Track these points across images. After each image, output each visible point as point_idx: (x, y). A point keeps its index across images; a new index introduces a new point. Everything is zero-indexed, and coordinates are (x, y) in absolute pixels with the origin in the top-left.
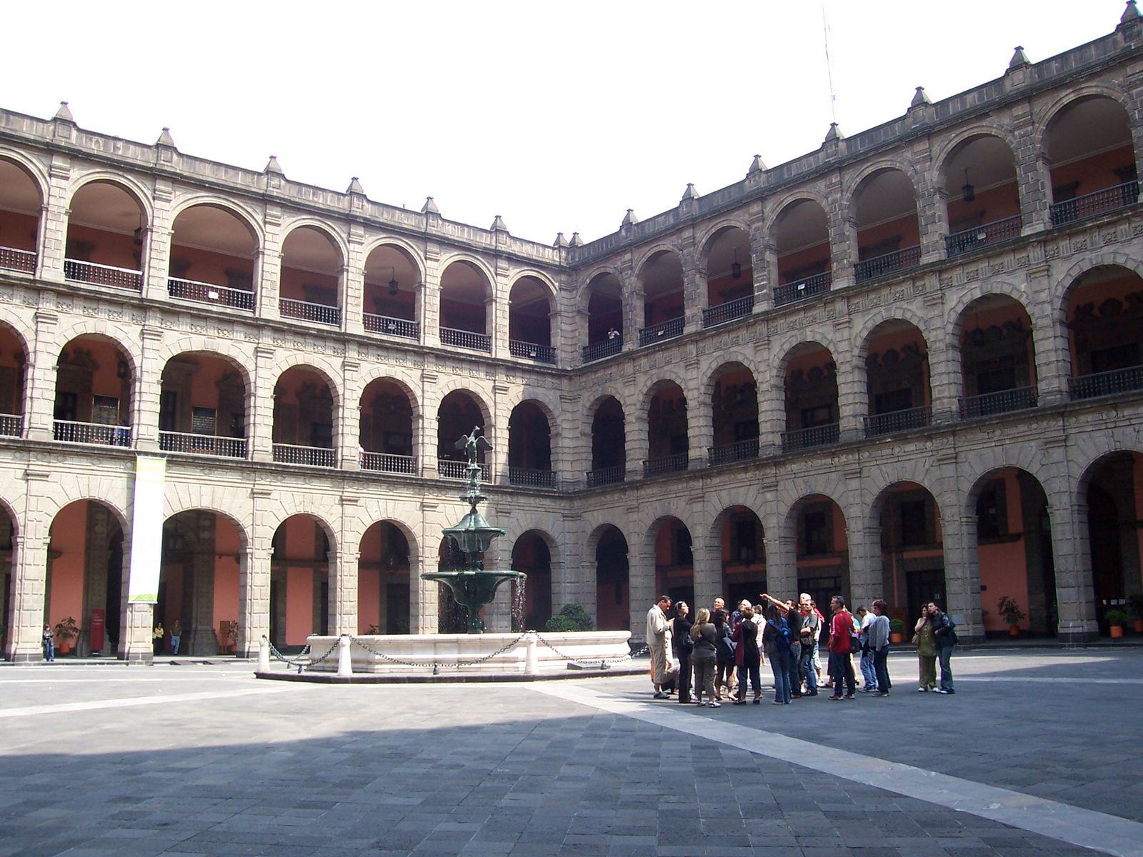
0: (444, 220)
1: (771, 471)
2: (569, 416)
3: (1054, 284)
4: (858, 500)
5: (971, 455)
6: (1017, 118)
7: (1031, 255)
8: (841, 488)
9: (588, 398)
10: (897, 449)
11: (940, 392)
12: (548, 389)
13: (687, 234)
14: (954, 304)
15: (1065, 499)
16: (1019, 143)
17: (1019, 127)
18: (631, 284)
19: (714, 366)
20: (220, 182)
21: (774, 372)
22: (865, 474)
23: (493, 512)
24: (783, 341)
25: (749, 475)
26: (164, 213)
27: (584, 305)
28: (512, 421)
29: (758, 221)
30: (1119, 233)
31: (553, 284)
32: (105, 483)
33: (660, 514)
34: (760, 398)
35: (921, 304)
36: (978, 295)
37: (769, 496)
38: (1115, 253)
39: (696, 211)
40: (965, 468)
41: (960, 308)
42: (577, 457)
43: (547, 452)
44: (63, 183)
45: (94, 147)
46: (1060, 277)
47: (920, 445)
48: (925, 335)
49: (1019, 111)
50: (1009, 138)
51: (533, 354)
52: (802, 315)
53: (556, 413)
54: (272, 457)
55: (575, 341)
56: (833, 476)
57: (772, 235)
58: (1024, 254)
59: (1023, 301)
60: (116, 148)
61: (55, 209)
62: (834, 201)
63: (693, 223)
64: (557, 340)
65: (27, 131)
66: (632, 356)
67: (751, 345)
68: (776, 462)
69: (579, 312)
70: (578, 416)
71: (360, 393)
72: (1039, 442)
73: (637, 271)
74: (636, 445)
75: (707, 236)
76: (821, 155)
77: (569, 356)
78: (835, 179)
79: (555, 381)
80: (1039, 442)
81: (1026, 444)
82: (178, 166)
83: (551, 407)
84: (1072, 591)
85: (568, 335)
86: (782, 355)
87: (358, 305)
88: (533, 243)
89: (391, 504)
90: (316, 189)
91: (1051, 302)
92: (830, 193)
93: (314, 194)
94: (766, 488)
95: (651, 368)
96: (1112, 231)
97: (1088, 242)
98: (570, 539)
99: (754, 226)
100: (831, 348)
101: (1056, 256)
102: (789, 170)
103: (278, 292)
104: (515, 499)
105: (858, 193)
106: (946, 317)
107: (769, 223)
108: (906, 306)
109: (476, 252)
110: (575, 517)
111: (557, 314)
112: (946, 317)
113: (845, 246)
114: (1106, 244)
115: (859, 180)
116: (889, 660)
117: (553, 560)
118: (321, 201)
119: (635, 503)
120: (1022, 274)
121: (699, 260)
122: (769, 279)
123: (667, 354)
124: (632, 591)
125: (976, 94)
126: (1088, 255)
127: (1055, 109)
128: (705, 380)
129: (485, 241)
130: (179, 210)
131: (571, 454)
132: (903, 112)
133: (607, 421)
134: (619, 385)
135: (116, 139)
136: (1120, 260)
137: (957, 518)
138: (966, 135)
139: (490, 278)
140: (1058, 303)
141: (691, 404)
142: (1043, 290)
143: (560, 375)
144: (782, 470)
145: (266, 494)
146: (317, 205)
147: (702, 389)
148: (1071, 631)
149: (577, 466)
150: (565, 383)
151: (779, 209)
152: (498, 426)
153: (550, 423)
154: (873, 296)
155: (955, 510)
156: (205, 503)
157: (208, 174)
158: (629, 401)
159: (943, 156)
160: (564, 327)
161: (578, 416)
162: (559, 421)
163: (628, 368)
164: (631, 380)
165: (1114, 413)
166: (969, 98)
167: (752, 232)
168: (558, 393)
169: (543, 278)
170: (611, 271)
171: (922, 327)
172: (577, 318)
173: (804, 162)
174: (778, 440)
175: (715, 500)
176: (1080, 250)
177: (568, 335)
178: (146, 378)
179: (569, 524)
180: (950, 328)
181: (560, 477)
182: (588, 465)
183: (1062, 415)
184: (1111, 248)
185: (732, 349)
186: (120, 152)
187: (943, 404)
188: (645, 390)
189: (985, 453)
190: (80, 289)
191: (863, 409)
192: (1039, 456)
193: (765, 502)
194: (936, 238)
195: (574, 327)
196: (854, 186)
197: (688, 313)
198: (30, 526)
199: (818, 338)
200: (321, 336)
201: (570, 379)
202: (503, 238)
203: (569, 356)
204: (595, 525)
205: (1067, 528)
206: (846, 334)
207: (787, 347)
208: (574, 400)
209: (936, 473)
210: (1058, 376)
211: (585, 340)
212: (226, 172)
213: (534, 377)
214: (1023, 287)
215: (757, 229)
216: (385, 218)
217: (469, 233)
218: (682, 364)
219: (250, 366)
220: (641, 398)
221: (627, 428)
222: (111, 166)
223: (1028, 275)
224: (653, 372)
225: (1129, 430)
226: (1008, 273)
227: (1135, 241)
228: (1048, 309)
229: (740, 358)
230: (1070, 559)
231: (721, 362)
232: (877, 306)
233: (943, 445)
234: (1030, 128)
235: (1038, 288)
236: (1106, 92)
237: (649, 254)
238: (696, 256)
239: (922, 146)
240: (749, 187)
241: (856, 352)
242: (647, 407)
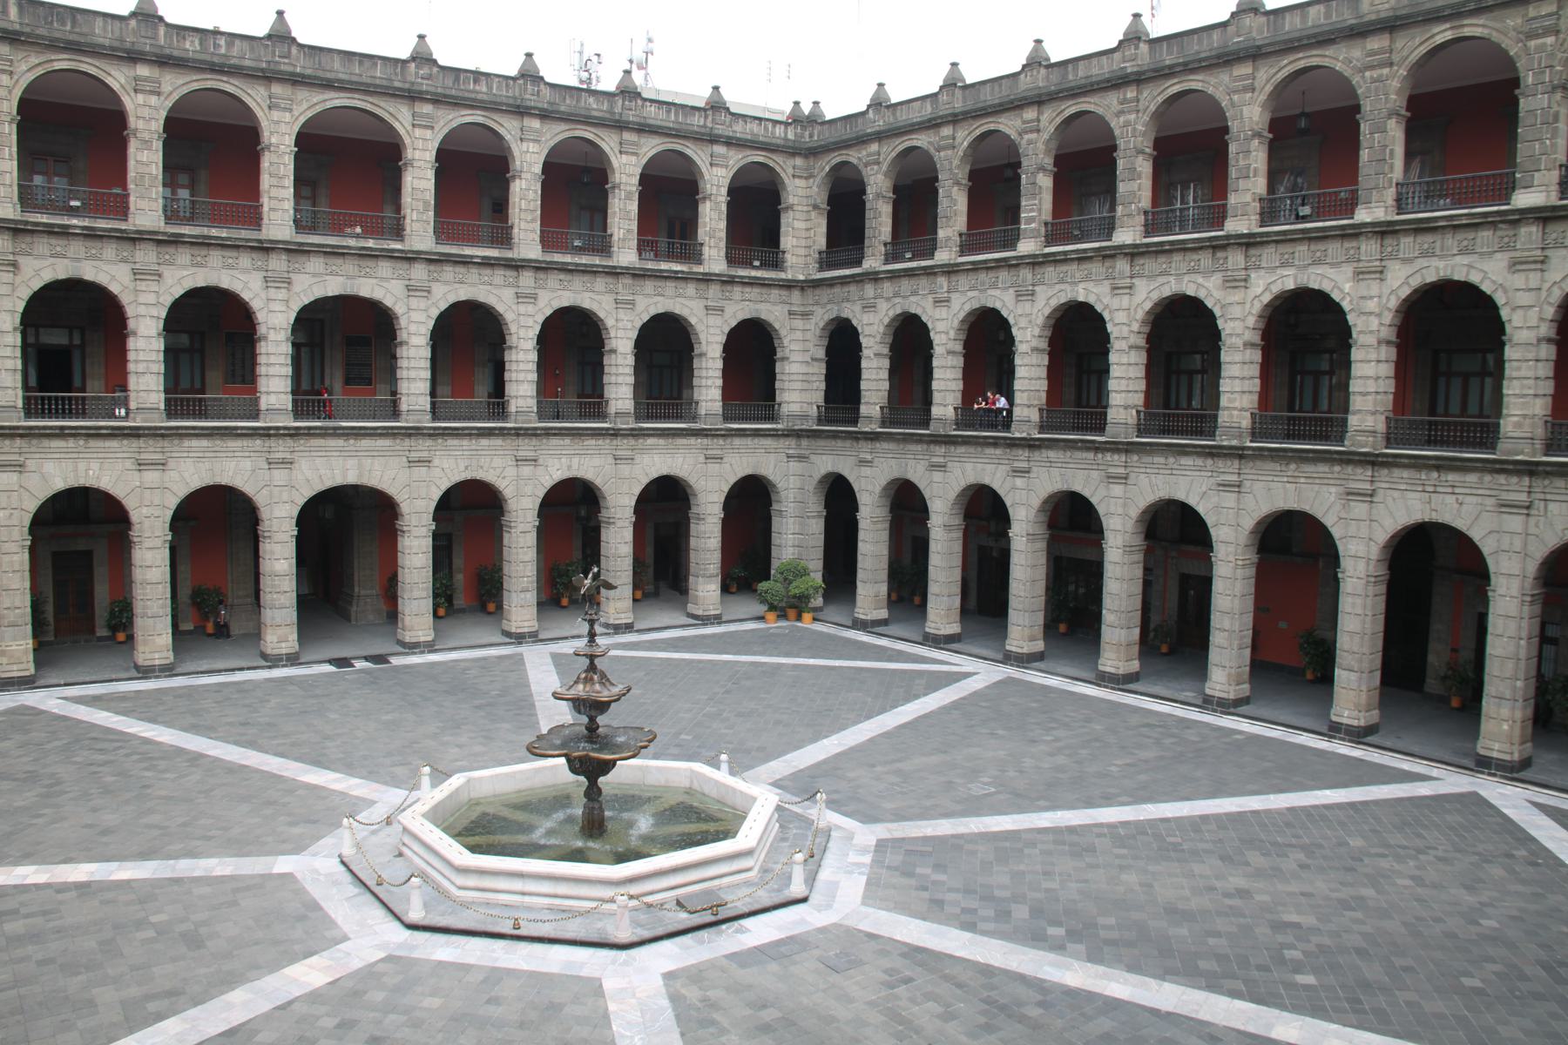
0: (646, 100)
1: (1023, 454)
2: (799, 335)
3: (1386, 291)
4: (1120, 511)
6: (1372, 53)
7: (1363, 248)
8: (1102, 492)
9: (822, 316)
10: (1171, 460)
11: (1230, 400)
12: (774, 304)
13: (946, 131)
14: (1259, 290)
15: (1361, 566)
16: (1368, 89)
17: (1372, 67)
18: (878, 186)
19: (967, 308)
20: (355, 79)
21: (1037, 331)
22: (1132, 475)
23: (702, 459)
24: (1052, 293)
25: (998, 451)
26: (280, 127)
27: (822, 198)
28: (727, 348)
29: (1031, 132)
30: (1479, 241)
31: (786, 168)
32: (235, 466)
33: (896, 474)
34: (1018, 361)
35: (1220, 281)
36: (1290, 285)
37: (1019, 482)
38: (1470, 266)
39: (959, 105)
40: (1248, 500)
41: (1267, 298)
42: (806, 386)
43: (772, 377)
44: (153, 100)
45: (191, 46)
46: (1396, 284)
48: (1220, 323)
49: (1376, 43)
50: (1355, 80)
51: (757, 263)
52: (1074, 266)
53: (783, 332)
54: (429, 417)
55: (810, 242)
56: (1095, 474)
57: (1047, 152)
58: (1354, 244)
59: (1346, 305)
60: (216, 46)
61: (146, 136)
62: (1127, 124)
63: (955, 119)
64: (787, 241)
65: (102, 35)
66: (874, 277)
67: (1011, 291)
68: (1030, 444)
69: (815, 207)
70: (809, 336)
71: (538, 328)
72: (1341, 489)
73: (884, 168)
74: (873, 386)
75: (970, 139)
76: (1117, 56)
77: (801, 260)
78: (1131, 93)
79: (784, 292)
80: (1341, 489)
81: (1325, 488)
82: (301, 66)
83: (777, 326)
84: (1353, 676)
85: (802, 232)
86: (1047, 311)
87: (533, 220)
88: (760, 119)
89: (576, 460)
90: (478, 75)
91: (1379, 315)
92: (1121, 112)
93: (475, 81)
94: (1017, 472)
95: (896, 295)
96: (1471, 235)
97: (1438, 244)
98: (793, 482)
99: (1026, 137)
100: (1106, 316)
101: (1393, 257)
103: (431, 213)
104: (729, 440)
105: (1158, 115)
106: (1248, 306)
107: (1046, 136)
108: (1200, 280)
109: (685, 137)
110: (801, 458)
111: (790, 208)
112: (1248, 306)
113: (1134, 185)
114: (1461, 252)
115: (1160, 99)
117: (775, 506)
118: (484, 89)
119: (869, 457)
120: (1348, 270)
121: (958, 167)
122: (1040, 210)
123: (913, 281)
124: (860, 558)
126: (1435, 262)
127: (1423, 49)
128: (956, 323)
129: (697, 121)
130: (302, 119)
131: (800, 382)
132: (1225, 17)
133: (842, 345)
134: (857, 308)
135: (216, 33)
136: (1474, 278)
137: (1231, 558)
138: (1301, 64)
139: (704, 170)
140: (1388, 318)
141: (938, 350)
142: (1371, 298)
143: (789, 285)
144: (1037, 453)
145: (427, 462)
146: (479, 97)
147: (952, 334)
148: (1345, 721)
149: (808, 397)
150: (796, 294)
151: (1059, 120)
152: (710, 355)
153: (776, 342)
154: (1162, 259)
155: (1231, 549)
156: (351, 479)
157: (338, 70)
158: (867, 330)
159: (1269, 88)
160: (797, 224)
161: (809, 336)
162: (786, 342)
163: (869, 290)
164: (869, 307)
165: (1435, 475)
167: (1024, 142)
168: (787, 307)
169: (772, 164)
170: (855, 161)
171: (1217, 312)
172: (813, 214)
173: (1095, 61)
174: (1035, 416)
175: (958, 472)
176: (1425, 254)
177: (802, 232)
178: (272, 336)
179: (794, 466)
180: (1251, 321)
181: (785, 409)
182: (819, 397)
183: (1373, 464)
184: (1465, 260)
185: (990, 292)
186: (223, 51)
187: (1231, 416)
188: (886, 320)
189: (1275, 490)
190: (183, 235)
191: (1139, 399)
192: (1338, 507)
193: (1014, 488)
194: (1248, 198)
195: (809, 225)
196: (1153, 108)
197: (941, 234)
198: (147, 523)
199: (1091, 300)
200: (487, 263)
201: (802, 289)
202: (723, 116)
203: (801, 260)
204: (823, 472)
205: (1359, 601)
206: (1125, 301)
207: (1054, 303)
208: (805, 315)
209: (1214, 499)
210: (1374, 413)
211: (821, 242)
212: (361, 63)
213: (756, 290)
214: (1347, 287)
215: (1030, 142)
216: (566, 105)
217: (676, 115)
218: (930, 298)
219: (399, 309)
220: (882, 329)
221: (864, 364)
222: (213, 71)
223: (1359, 274)
224: (897, 300)
225: (1450, 499)
226: (1332, 265)
227: (1498, 256)
228: (1374, 323)
229: (998, 306)
230: (1357, 639)
231: (976, 305)
232: (1164, 273)
233: (1229, 470)
234: (1386, 71)
235: (1365, 293)
237: (901, 148)
238: (956, 162)
239: (1244, 69)
240: (1025, 83)
241: (1136, 327)
242: (889, 340)
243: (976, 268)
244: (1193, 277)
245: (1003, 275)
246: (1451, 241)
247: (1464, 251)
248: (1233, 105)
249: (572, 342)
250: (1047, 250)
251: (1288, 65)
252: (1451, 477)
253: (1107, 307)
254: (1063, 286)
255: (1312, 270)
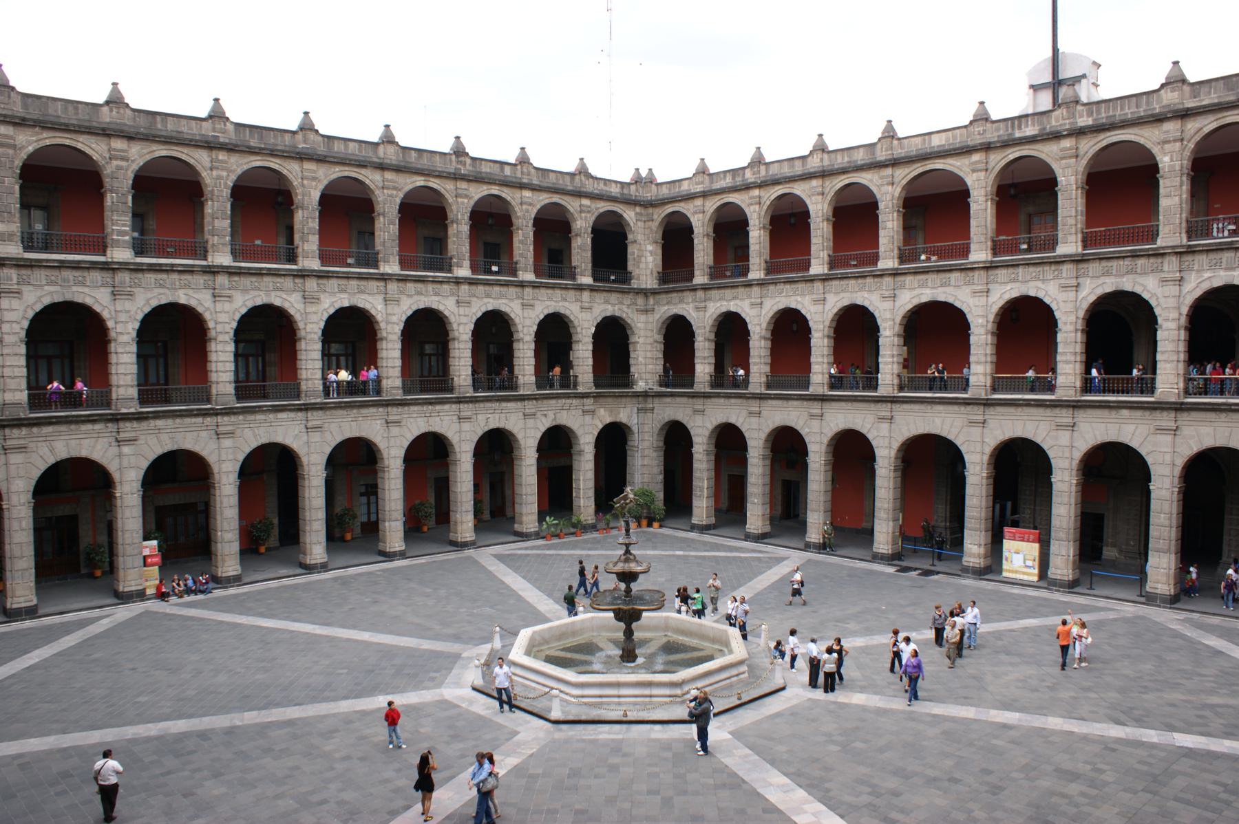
4: (231, 457)
5: (333, 425)
25: (98, 427)
36: (346, 304)
46: (405, 308)
47: (292, 415)
56: (204, 434)
102: (164, 122)
116: (121, 589)
125: (356, 145)
126: (423, 298)
136: (441, 308)
166: (351, 145)
176: (419, 293)
184: (437, 298)
214: (380, 307)
215: (119, 168)
236: (443, 191)
243: (62, 265)
244: (279, 293)
245: (96, 276)
246: (430, 287)
247: (437, 294)
248: (303, 186)
249: (267, 333)
250: (139, 260)
251: (337, 172)
252: (438, 407)
253: (208, 309)
254: (162, 291)
255: (358, 296)
